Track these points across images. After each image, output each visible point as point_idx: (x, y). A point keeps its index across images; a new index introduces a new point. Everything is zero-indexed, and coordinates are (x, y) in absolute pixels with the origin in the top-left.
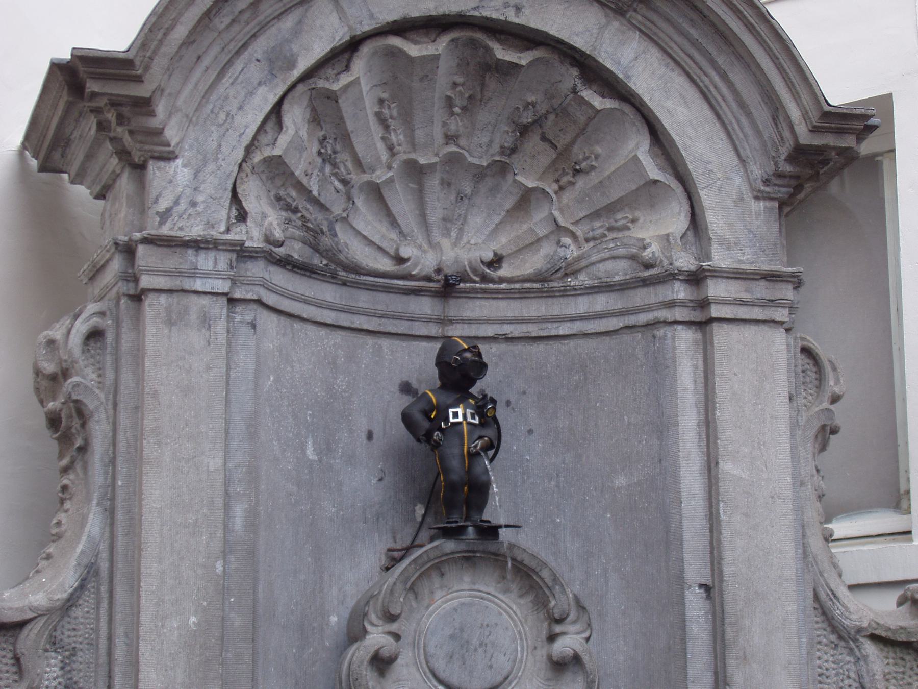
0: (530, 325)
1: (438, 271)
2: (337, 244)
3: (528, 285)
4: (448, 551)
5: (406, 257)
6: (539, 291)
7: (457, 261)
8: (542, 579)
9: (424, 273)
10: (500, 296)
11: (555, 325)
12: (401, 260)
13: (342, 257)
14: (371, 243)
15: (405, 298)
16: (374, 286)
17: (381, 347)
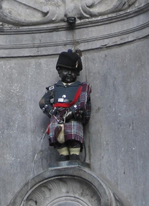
0: (116, 38)
1: (66, 15)
2: (2, 13)
3: (110, 16)
4: (46, 177)
5: (46, 12)
6: (116, 18)
7: (76, 8)
8: (95, 187)
9: (60, 18)
10: (100, 24)
11: (127, 35)
12: (45, 14)
13: (8, 19)
14: (29, 7)
15: (51, 34)
16: (29, 31)
17: (40, 64)
